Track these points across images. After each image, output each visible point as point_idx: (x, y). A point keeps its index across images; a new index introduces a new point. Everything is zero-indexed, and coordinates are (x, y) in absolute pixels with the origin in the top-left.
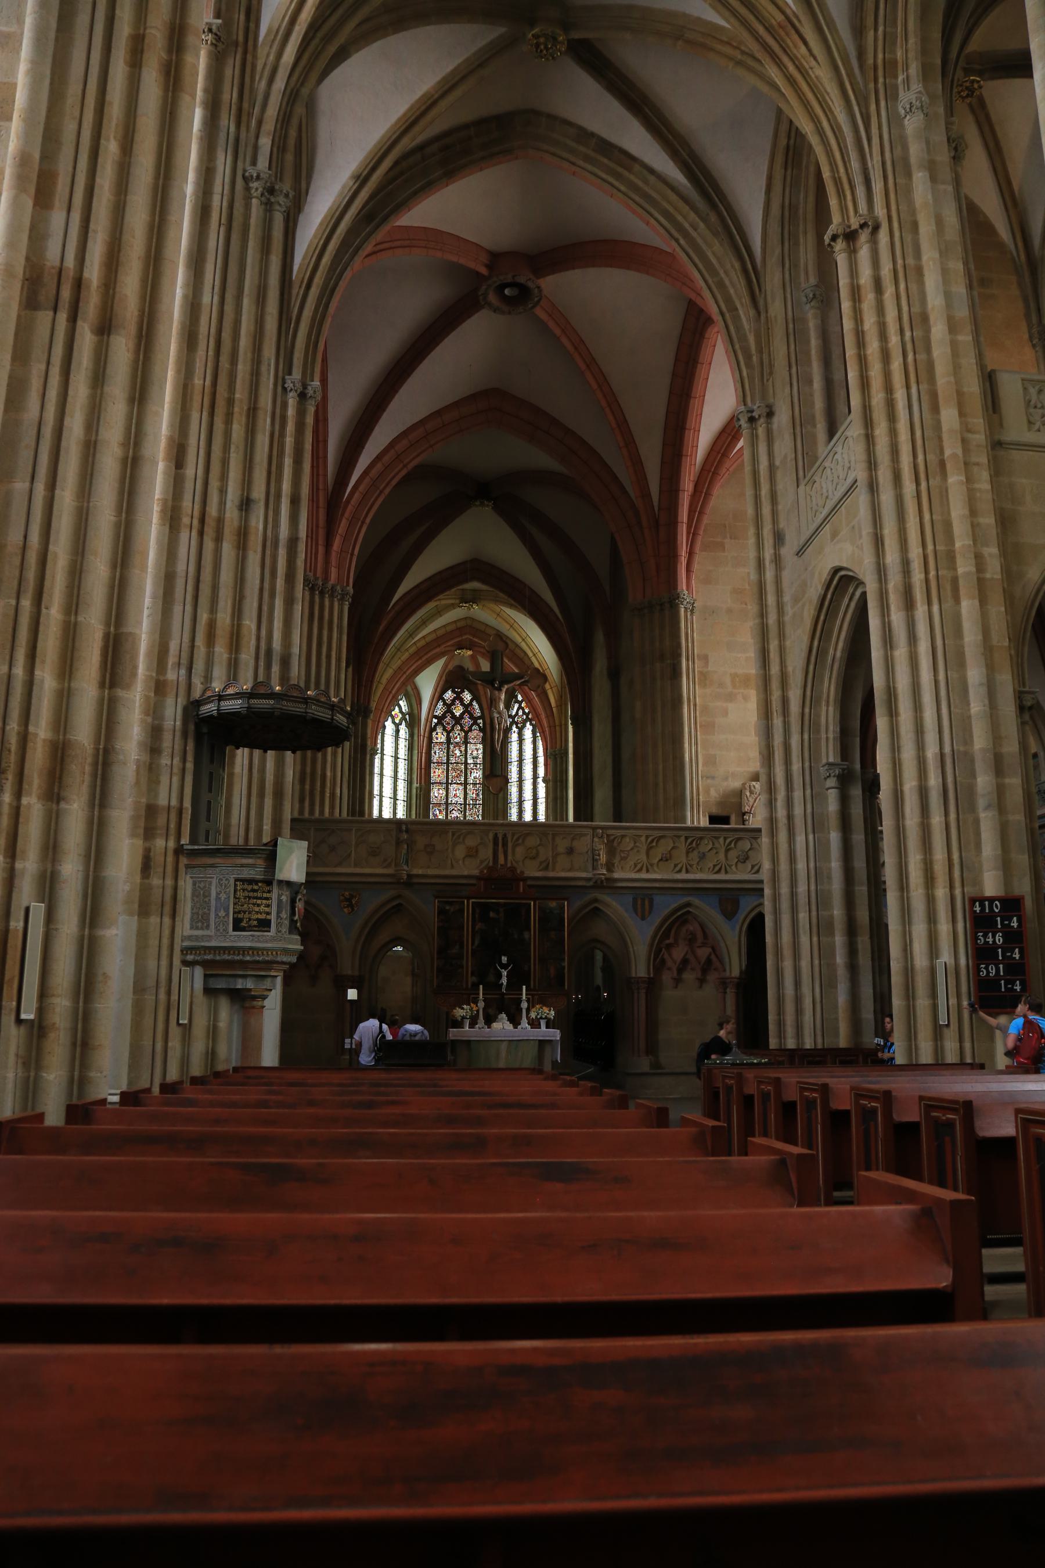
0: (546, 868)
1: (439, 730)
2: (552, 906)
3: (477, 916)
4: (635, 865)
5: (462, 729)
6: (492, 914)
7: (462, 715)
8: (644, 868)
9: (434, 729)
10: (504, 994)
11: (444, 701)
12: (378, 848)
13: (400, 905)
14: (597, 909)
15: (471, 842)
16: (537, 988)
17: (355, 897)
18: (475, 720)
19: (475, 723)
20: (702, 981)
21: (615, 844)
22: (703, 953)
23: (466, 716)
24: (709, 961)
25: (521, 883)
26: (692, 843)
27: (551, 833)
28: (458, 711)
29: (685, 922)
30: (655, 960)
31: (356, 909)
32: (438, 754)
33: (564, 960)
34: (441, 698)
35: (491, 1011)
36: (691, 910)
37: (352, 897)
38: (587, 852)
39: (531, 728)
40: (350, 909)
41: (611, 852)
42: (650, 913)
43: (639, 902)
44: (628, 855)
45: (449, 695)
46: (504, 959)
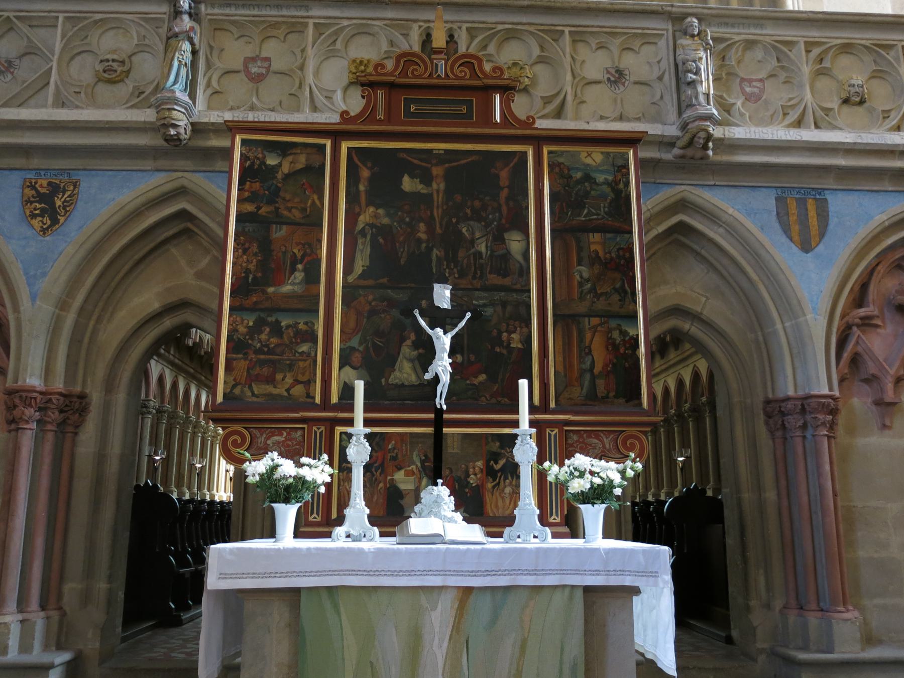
0: (559, 114)
2: (589, 161)
3: (362, 188)
6: (408, 184)
10: (439, 412)
12: (123, 62)
13: (183, 215)
14: (682, 228)
16: (553, 405)
17: (64, 192)
27: (567, 30)
31: (62, 219)
33: (635, 317)
35: (403, 480)
37: (55, 189)
38: (660, 78)
40: (47, 220)
42: (822, 235)
43: (793, 207)
44: (762, 90)
46: (443, 296)
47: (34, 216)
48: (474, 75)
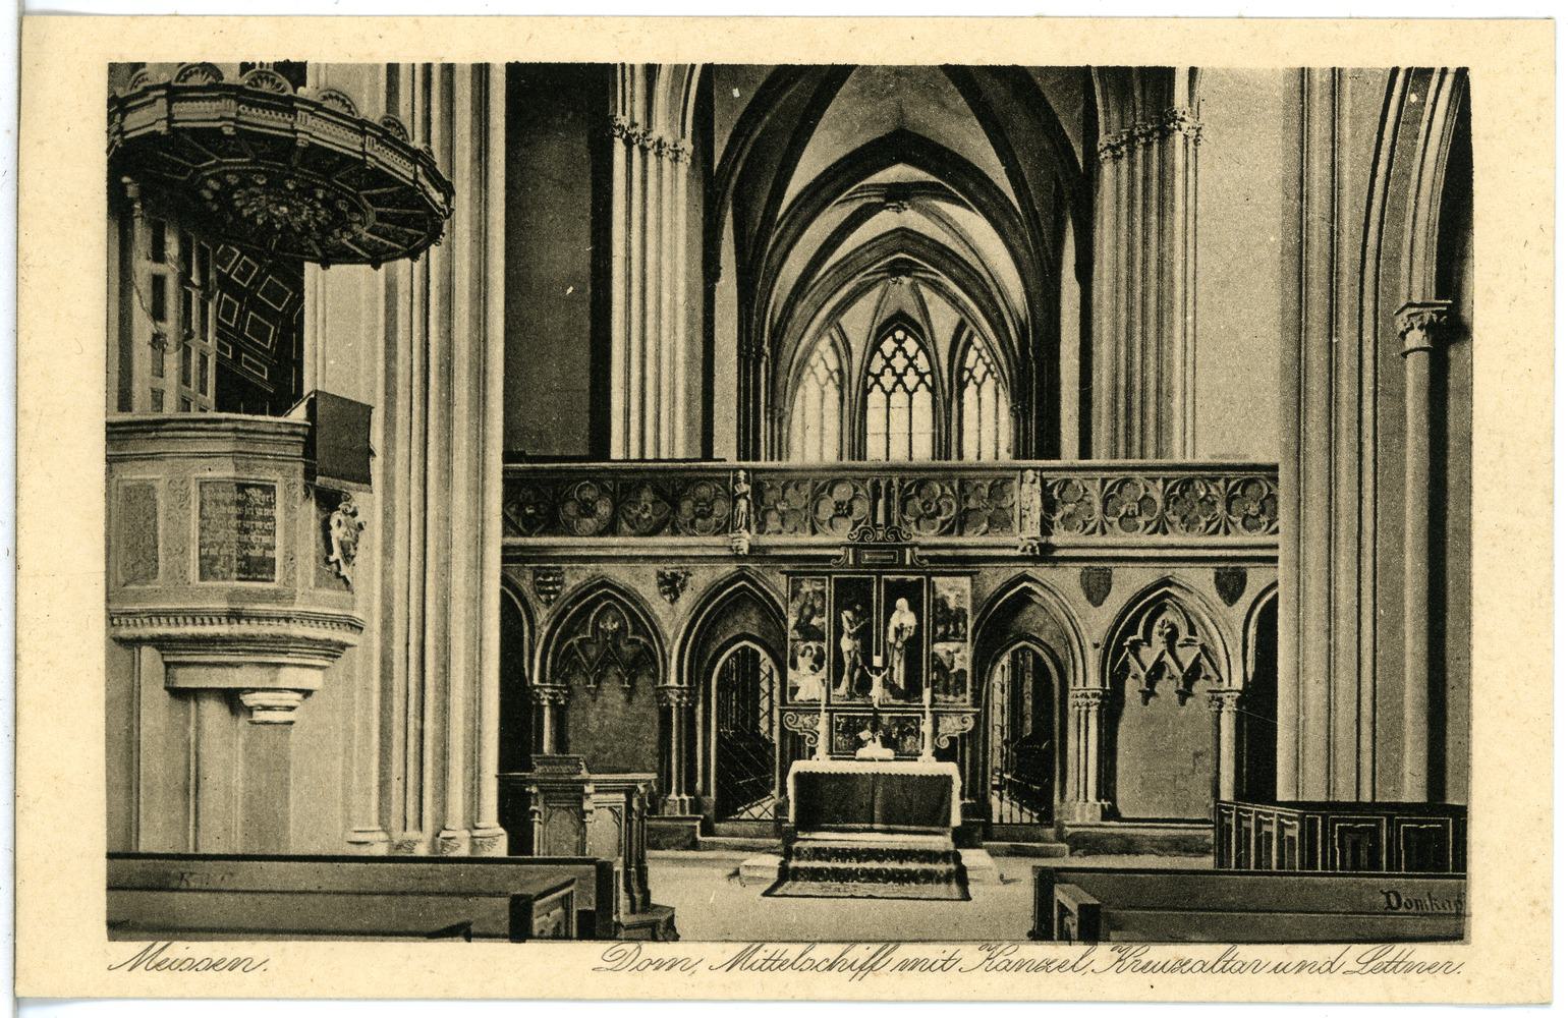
0: (949, 532)
1: (877, 388)
4: (1085, 526)
5: (906, 390)
7: (906, 369)
8: (1098, 529)
9: (870, 390)
11: (882, 353)
15: (842, 492)
18: (922, 376)
19: (922, 380)
20: (1184, 695)
21: (1055, 492)
22: (1187, 656)
23: (911, 371)
24: (1196, 667)
25: (908, 551)
26: (1173, 489)
28: (899, 363)
29: (1161, 609)
30: (1113, 665)
32: (875, 420)
34: (876, 347)
36: (1171, 590)
39: (993, 382)
41: (1049, 506)
45: (888, 346)
47: (665, 593)
48: (898, 540)
